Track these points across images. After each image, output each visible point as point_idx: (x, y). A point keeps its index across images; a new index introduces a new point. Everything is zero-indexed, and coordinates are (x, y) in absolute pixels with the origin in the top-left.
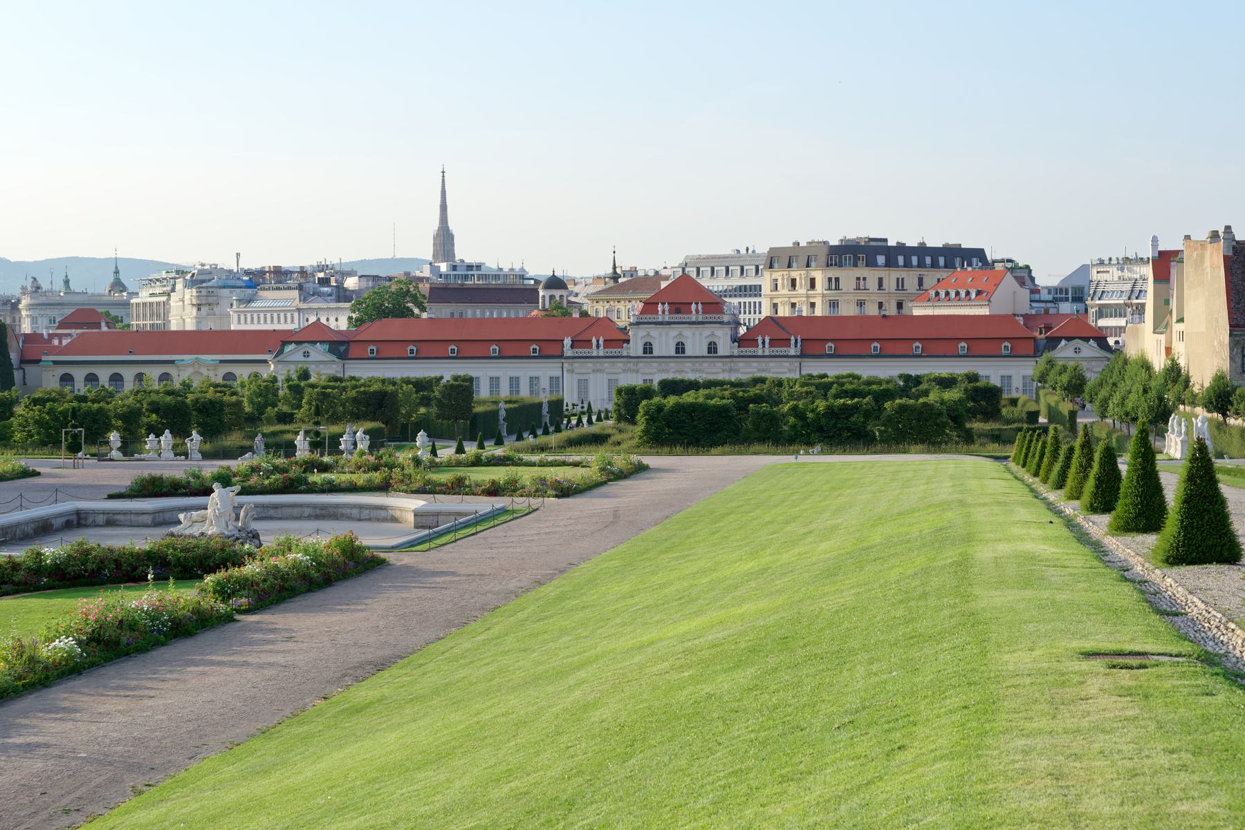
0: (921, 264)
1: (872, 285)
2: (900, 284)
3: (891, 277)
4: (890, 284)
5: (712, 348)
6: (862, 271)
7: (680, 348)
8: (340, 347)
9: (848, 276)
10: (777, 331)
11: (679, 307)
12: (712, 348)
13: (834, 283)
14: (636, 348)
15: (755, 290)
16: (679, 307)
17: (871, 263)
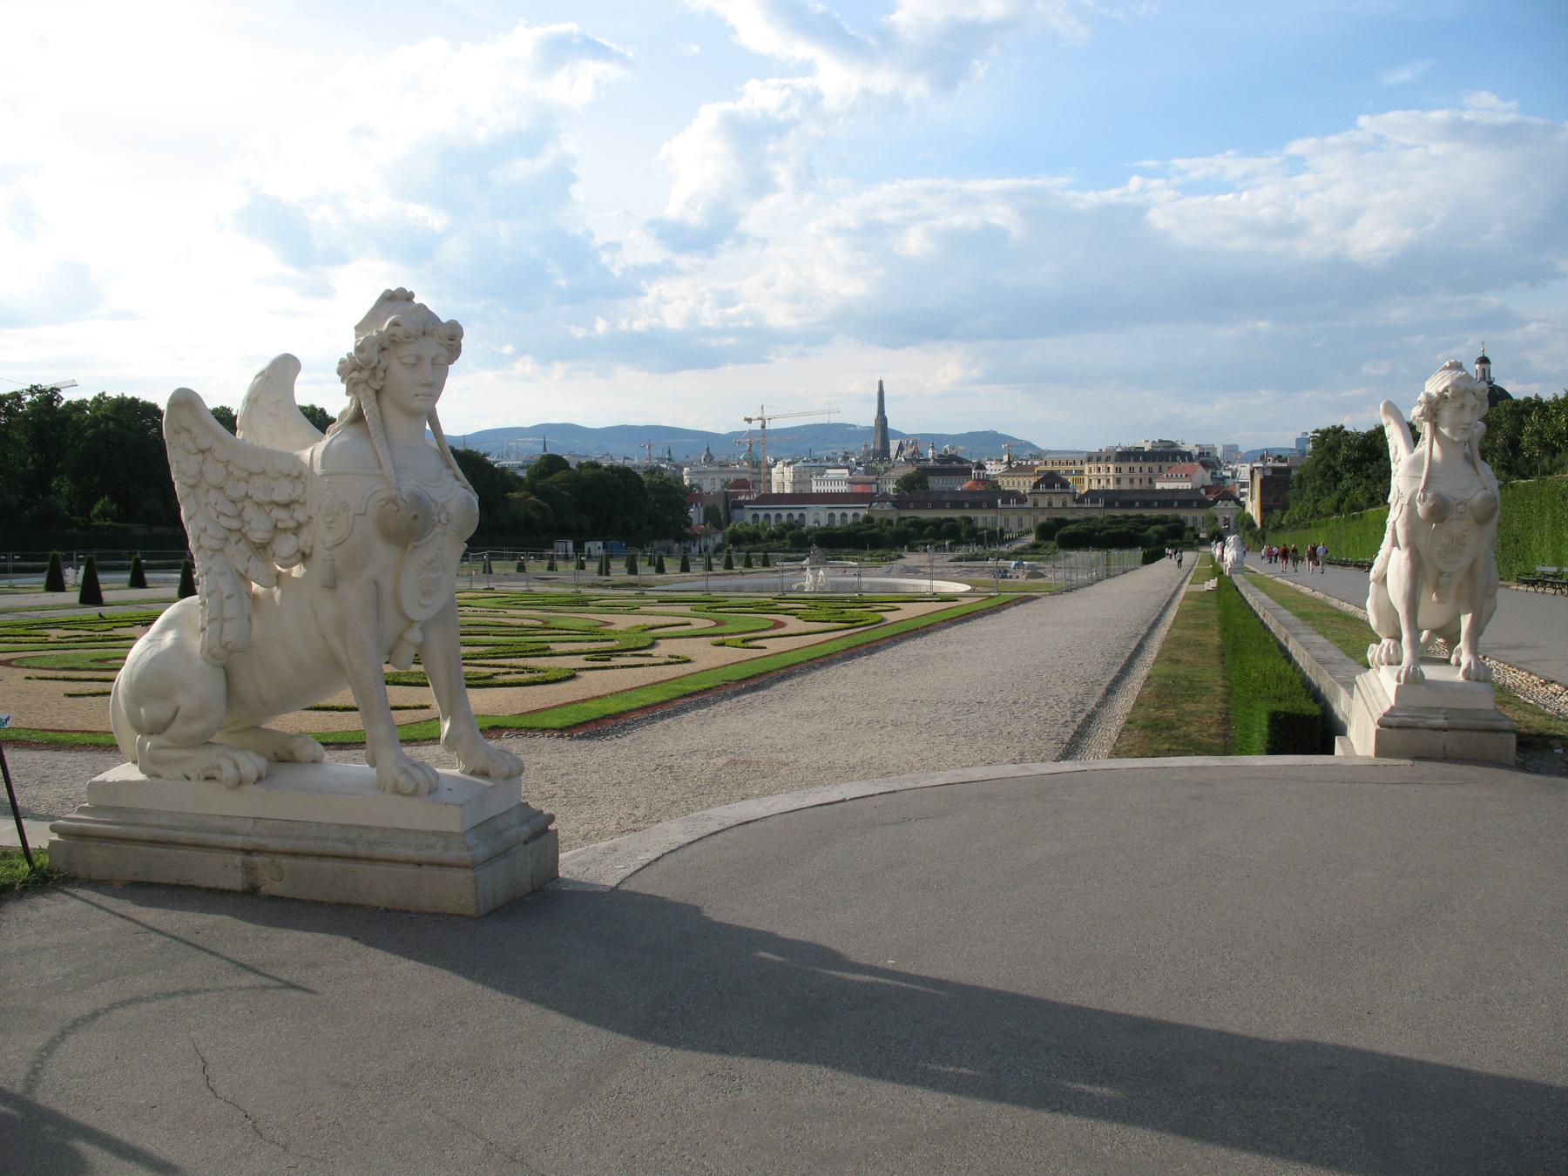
1: (1137, 470)
2: (1150, 470)
4: (1145, 470)
5: (1064, 504)
6: (1132, 464)
7: (1050, 504)
9: (1125, 467)
12: (1064, 504)
13: (1118, 470)
14: (1029, 504)
17: (1137, 460)
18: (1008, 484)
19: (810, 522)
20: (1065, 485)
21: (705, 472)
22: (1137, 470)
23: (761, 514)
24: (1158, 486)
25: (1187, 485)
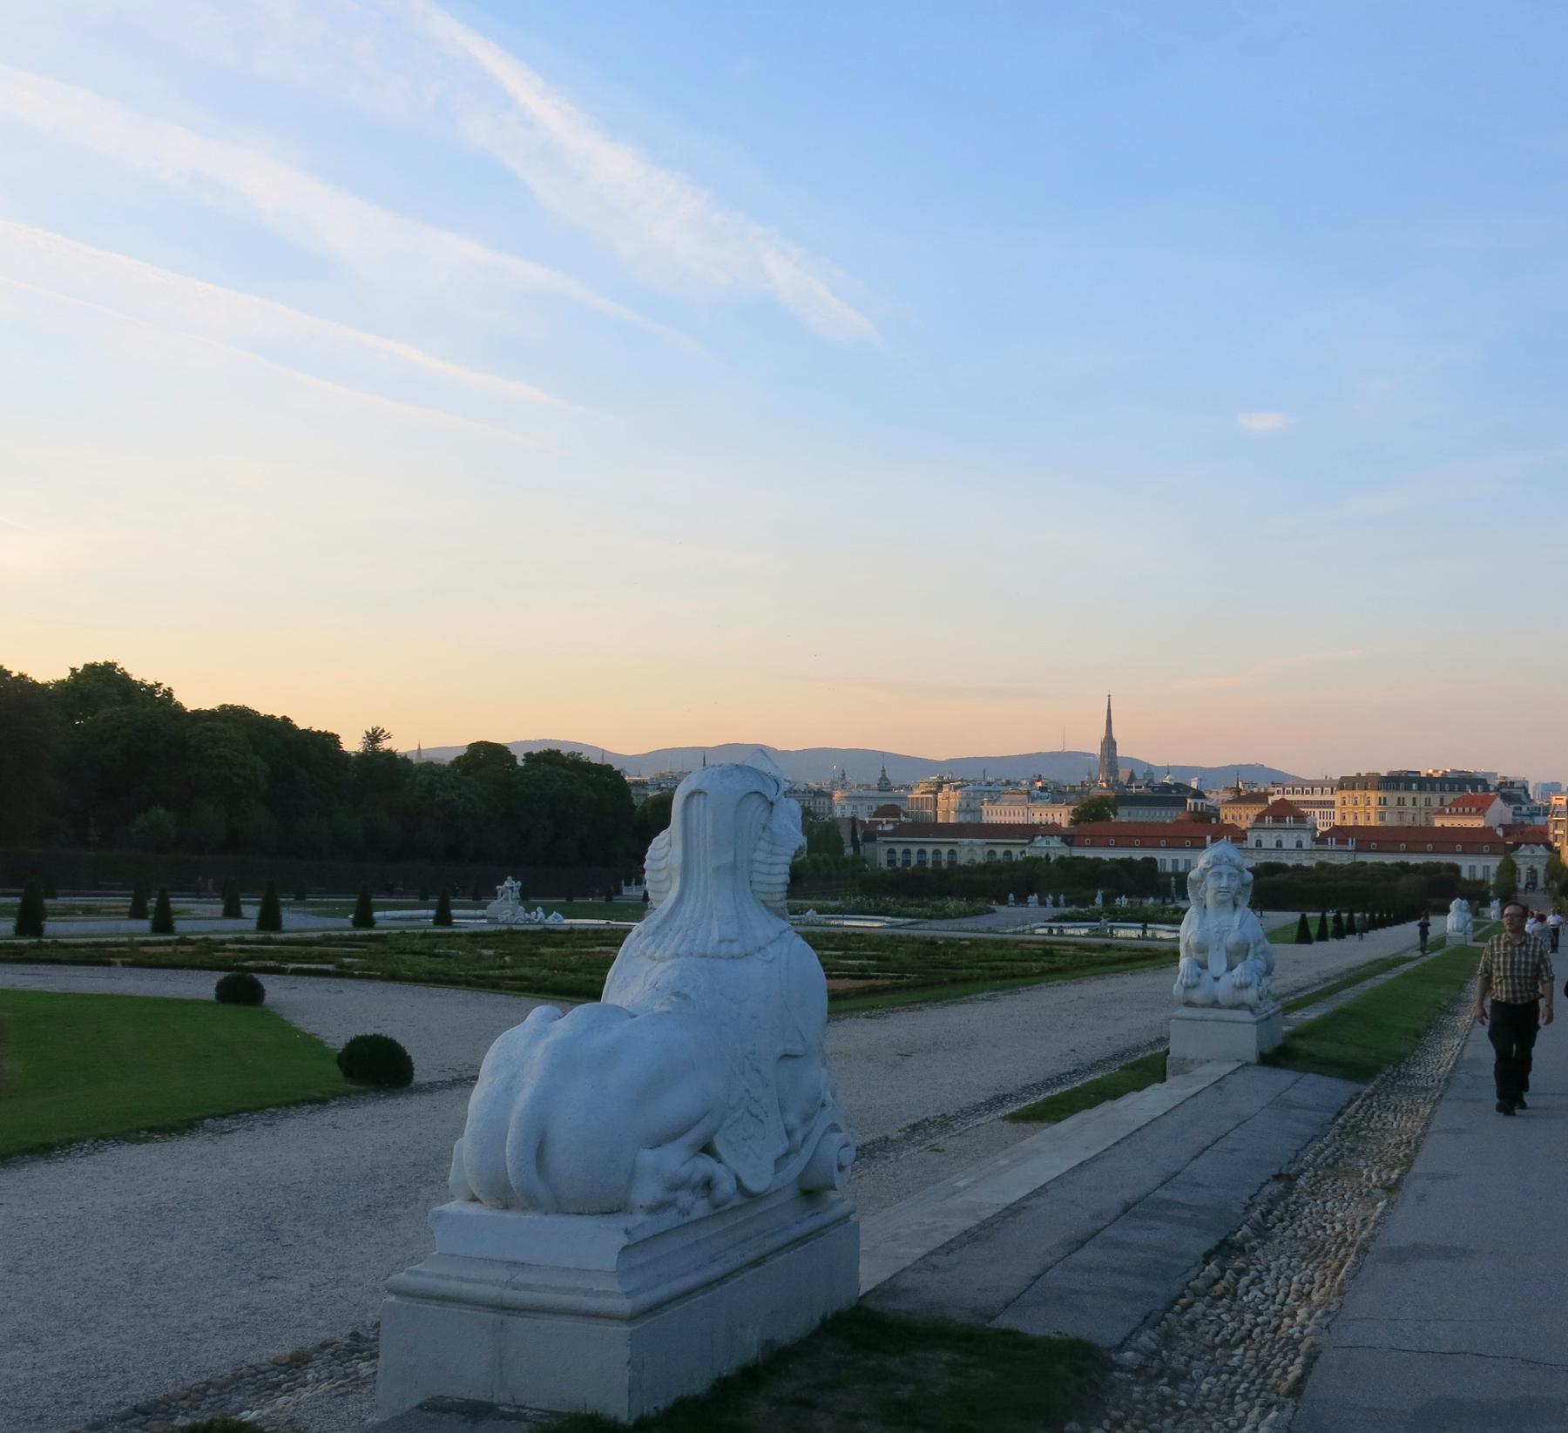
0: (1442, 789)
1: (1409, 802)
2: (1428, 802)
3: (1422, 797)
4: (1421, 802)
5: (1299, 844)
7: (1279, 844)
8: (1069, 839)
9: (1392, 797)
10: (1340, 834)
11: (1278, 819)
12: (1299, 844)
14: (1251, 843)
15: (1331, 804)
16: (1278, 819)
17: (1408, 789)
18: (1228, 815)
19: (963, 859)
20: (1301, 818)
21: (861, 798)
22: (1409, 802)
23: (899, 849)
24: (1438, 823)
25: (1477, 823)
